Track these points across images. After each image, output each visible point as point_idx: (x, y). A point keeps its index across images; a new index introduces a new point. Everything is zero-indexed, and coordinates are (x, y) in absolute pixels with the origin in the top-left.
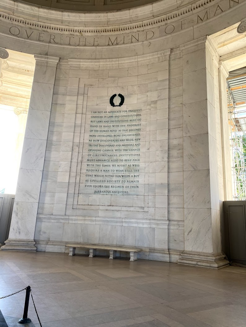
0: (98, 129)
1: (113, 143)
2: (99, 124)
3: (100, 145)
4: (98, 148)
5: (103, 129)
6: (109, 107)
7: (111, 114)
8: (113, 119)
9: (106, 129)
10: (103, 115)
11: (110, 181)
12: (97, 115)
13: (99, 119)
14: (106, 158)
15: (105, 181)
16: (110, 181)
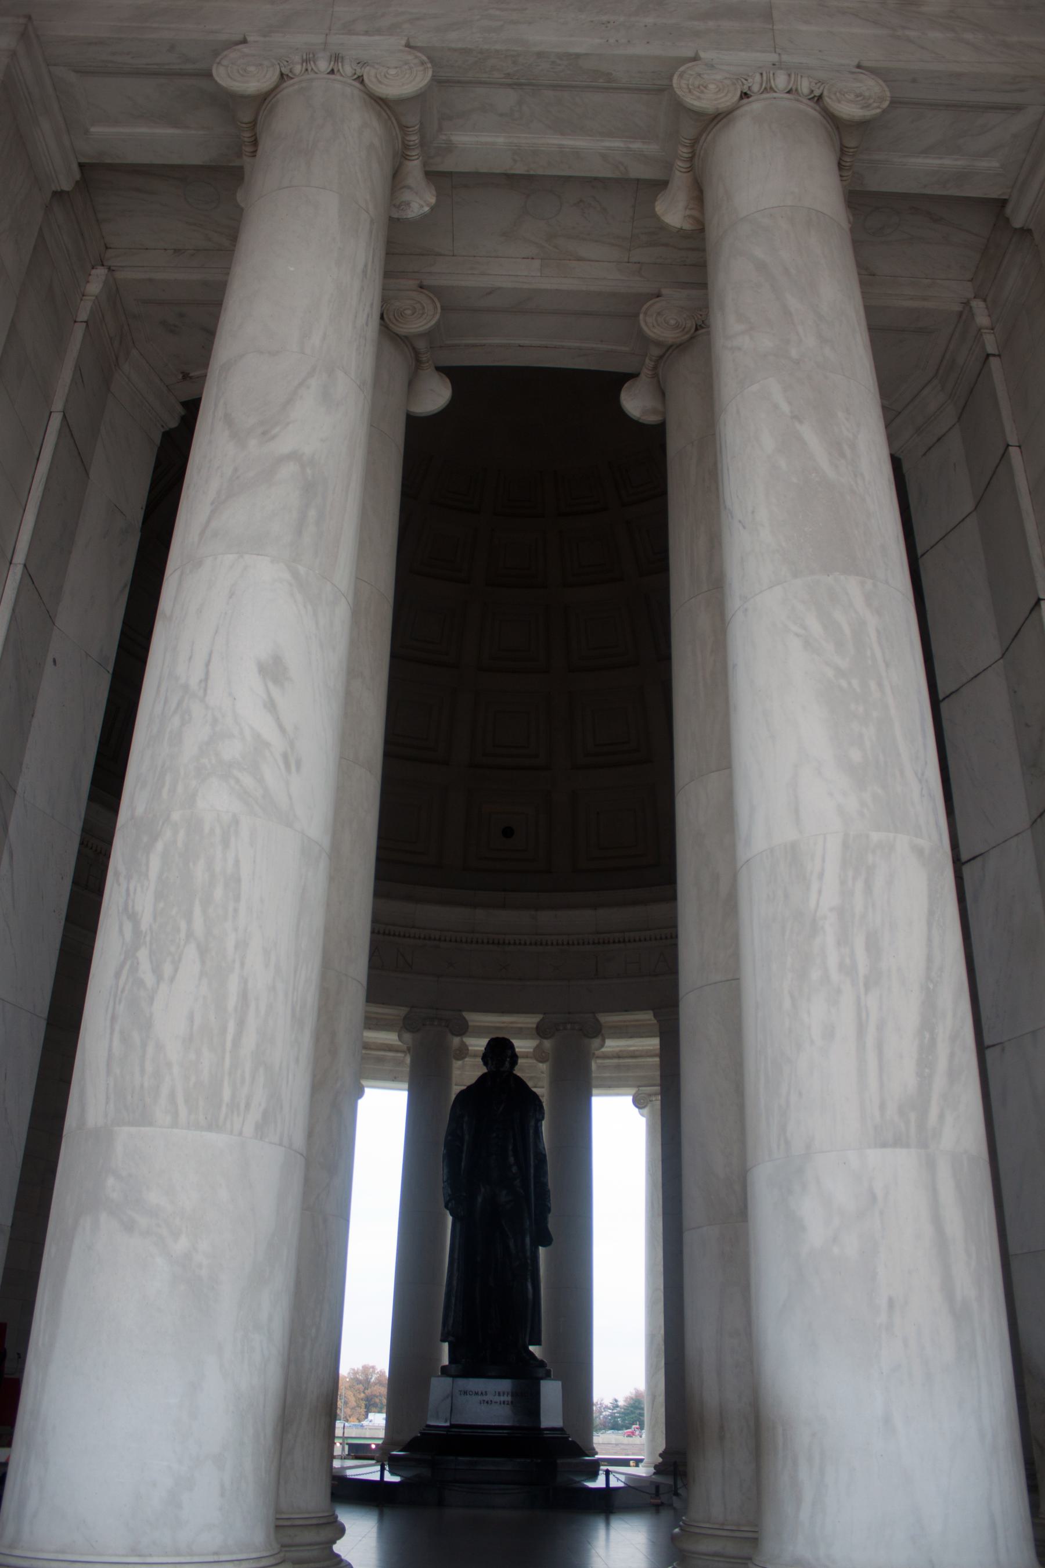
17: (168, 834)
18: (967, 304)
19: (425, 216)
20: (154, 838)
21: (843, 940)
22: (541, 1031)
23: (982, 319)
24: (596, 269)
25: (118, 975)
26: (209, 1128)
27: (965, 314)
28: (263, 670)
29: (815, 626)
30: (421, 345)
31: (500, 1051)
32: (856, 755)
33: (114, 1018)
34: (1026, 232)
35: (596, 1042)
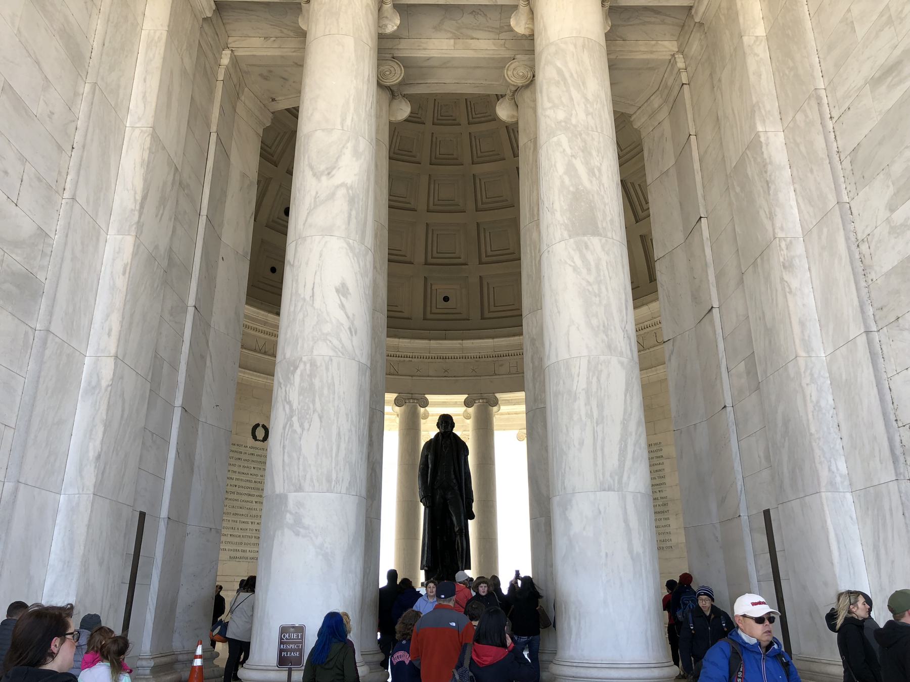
0: (235, 469)
1: (253, 492)
2: (238, 463)
3: (238, 493)
4: (235, 497)
5: (242, 470)
6: (250, 441)
7: (252, 451)
8: (255, 458)
9: (245, 471)
10: (242, 449)
11: (248, 544)
12: (235, 448)
13: (238, 456)
14: (244, 512)
15: (241, 543)
16: (248, 544)
17: (301, 366)
18: (673, 55)
19: (395, 31)
20: (296, 368)
21: (588, 403)
22: (468, 404)
23: (681, 64)
24: (482, 46)
25: (284, 428)
26: (328, 491)
27: (672, 61)
28: (337, 291)
29: (578, 262)
30: (394, 89)
31: (446, 422)
32: (594, 322)
33: (284, 447)
34: (701, 24)
35: (495, 409)
